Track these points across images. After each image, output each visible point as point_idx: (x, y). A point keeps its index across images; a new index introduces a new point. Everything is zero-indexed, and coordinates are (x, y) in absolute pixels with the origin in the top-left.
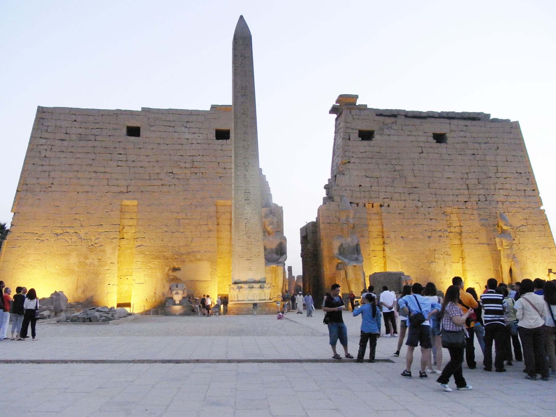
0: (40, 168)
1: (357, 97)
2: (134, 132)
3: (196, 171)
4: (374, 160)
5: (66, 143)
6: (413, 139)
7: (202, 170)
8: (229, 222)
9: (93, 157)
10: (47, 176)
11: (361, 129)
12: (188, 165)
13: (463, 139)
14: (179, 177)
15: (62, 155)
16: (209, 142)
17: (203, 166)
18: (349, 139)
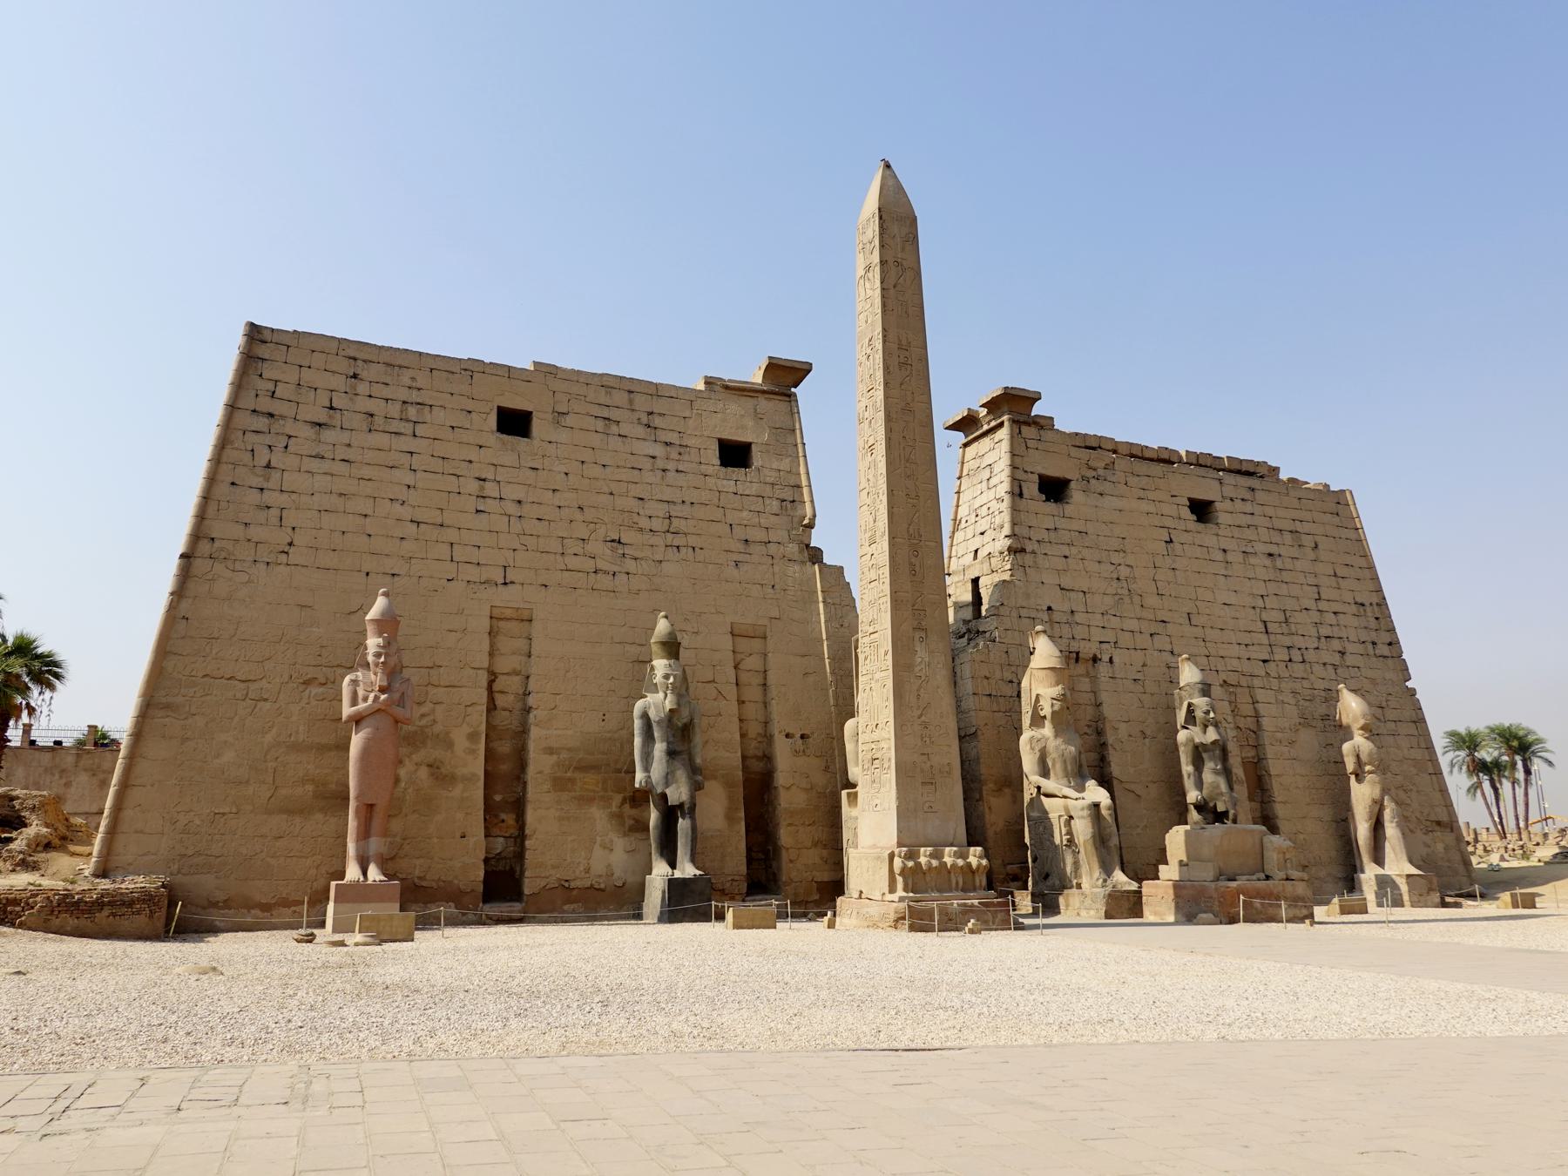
0: (254, 497)
1: (1033, 398)
2: (514, 423)
3: (678, 541)
4: (1074, 550)
5: (329, 435)
6: (1152, 509)
7: (692, 541)
8: (758, 680)
9: (409, 478)
10: (276, 521)
11: (1043, 472)
12: (657, 524)
13: (1248, 520)
14: (637, 554)
15: (315, 465)
18: (1021, 495)
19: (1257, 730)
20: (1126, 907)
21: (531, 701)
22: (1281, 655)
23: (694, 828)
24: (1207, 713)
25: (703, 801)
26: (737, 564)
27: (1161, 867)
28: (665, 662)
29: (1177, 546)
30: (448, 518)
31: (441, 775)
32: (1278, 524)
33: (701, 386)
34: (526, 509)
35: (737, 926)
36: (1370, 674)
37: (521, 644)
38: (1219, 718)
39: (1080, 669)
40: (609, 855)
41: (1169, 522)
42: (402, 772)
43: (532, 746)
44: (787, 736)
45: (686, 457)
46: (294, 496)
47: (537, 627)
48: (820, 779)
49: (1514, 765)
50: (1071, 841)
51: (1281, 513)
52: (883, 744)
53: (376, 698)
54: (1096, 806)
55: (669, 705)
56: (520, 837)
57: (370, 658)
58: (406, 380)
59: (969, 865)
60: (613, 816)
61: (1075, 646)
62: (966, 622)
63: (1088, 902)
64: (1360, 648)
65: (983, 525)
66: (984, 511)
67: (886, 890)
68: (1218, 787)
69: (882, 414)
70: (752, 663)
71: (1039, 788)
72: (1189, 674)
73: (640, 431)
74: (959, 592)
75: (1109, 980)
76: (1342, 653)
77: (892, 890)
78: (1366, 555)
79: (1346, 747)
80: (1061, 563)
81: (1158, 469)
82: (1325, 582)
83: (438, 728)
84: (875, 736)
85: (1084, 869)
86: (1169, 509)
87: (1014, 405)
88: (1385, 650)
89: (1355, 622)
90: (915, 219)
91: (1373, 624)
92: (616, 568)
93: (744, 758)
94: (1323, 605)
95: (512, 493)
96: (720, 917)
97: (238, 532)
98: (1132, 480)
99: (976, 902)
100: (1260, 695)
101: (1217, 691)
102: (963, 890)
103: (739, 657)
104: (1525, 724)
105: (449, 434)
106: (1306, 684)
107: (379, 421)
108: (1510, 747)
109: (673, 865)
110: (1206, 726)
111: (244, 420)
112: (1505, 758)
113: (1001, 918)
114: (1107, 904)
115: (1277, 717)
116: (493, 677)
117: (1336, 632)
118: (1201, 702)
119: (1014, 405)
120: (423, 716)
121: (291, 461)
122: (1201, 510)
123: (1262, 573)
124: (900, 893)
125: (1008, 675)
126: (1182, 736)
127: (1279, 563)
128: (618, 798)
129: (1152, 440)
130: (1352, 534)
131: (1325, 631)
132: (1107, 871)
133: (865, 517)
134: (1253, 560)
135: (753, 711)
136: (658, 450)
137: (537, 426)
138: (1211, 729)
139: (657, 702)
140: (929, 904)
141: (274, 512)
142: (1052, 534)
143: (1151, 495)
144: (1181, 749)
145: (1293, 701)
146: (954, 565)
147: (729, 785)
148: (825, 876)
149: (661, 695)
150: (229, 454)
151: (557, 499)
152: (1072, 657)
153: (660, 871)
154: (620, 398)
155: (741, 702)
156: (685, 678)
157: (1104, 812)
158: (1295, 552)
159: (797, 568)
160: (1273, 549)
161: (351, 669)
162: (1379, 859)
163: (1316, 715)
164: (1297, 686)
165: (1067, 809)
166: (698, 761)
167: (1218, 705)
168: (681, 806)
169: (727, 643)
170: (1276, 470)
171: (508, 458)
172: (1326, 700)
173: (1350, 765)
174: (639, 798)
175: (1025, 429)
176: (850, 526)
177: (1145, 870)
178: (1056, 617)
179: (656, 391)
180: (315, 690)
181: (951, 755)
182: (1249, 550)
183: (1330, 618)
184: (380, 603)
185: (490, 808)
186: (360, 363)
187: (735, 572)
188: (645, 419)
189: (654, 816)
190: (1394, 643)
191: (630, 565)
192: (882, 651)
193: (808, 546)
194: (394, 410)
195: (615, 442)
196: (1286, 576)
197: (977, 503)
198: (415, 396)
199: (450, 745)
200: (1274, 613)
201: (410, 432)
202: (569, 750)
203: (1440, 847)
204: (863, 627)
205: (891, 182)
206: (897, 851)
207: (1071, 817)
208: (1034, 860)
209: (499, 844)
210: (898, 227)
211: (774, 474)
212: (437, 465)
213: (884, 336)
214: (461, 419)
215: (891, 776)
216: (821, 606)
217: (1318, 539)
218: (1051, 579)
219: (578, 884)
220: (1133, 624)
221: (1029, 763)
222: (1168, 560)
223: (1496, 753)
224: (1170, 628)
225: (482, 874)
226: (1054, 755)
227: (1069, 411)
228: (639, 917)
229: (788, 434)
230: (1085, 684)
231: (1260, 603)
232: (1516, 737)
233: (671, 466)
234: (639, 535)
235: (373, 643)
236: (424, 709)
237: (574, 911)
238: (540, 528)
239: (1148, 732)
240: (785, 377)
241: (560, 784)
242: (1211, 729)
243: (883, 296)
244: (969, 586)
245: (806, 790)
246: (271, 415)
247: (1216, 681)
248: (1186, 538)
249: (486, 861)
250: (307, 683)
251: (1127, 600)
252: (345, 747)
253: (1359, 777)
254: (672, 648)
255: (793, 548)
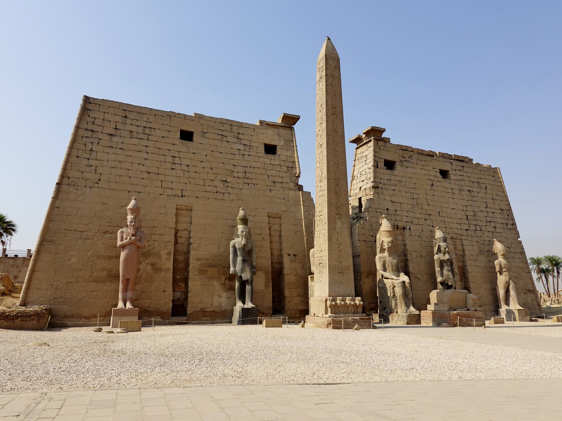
0: (85, 162)
1: (383, 131)
2: (187, 136)
3: (249, 181)
4: (397, 188)
5: (115, 139)
6: (425, 172)
7: (254, 181)
8: (278, 234)
9: (146, 156)
10: (94, 171)
12: (240, 175)
13: (461, 178)
15: (109, 150)
16: (258, 154)
17: (254, 178)
18: (377, 167)
19: (463, 255)
20: (414, 320)
21: (191, 241)
22: (472, 228)
23: (252, 289)
24: (445, 248)
25: (255, 279)
26: (270, 190)
27: (428, 305)
28: (242, 226)
29: (435, 187)
30: (161, 171)
31: (156, 268)
32: (472, 179)
33: (258, 124)
34: (191, 168)
35: (267, 326)
36: (505, 235)
37: (188, 219)
38: (450, 251)
39: (399, 232)
40: (220, 299)
41: (432, 178)
42: (141, 267)
43: (191, 258)
44: (288, 255)
45: (252, 150)
46: (101, 162)
47: (194, 213)
48: (300, 271)
49: (553, 270)
50: (394, 296)
51: (473, 175)
52: (324, 258)
53: (130, 238)
54: (404, 282)
55: (243, 243)
56: (186, 292)
57: (128, 223)
58: (145, 119)
59: (356, 304)
60: (221, 284)
61: (396, 223)
62: (356, 214)
63: (400, 318)
64: (501, 226)
65: (363, 178)
66: (364, 173)
67: (324, 313)
68: (449, 276)
69: (325, 133)
70: (276, 227)
71: (382, 276)
72: (439, 234)
73: (235, 140)
74: (354, 202)
75: (410, 351)
76: (495, 227)
77: (326, 313)
78: (504, 192)
79: (496, 262)
80: (392, 192)
81: (429, 158)
82: (489, 201)
83: (155, 250)
84: (321, 254)
85: (399, 306)
86: (432, 173)
87: (375, 133)
88: (511, 227)
89: (499, 216)
90: (339, 59)
91: (506, 217)
92: (224, 191)
93: (272, 263)
94: (488, 210)
95: (185, 162)
96: (261, 323)
97: (79, 175)
98: (419, 162)
99: (358, 318)
100: (465, 242)
101: (449, 241)
102: (354, 313)
103: (271, 225)
104: (558, 256)
105: (162, 140)
106: (482, 239)
107: (135, 134)
108: (552, 264)
109: (244, 303)
110: (445, 254)
111: (82, 132)
112: (550, 268)
113: (367, 324)
114: (408, 319)
115: (471, 250)
116: (177, 231)
117: (493, 220)
118: (443, 245)
119: (375, 133)
120: (149, 246)
121: (100, 149)
122: (444, 174)
123: (466, 197)
124: (329, 314)
125: (371, 234)
126: (436, 257)
127: (472, 194)
128: (224, 278)
129: (427, 148)
130: (499, 184)
131: (489, 219)
132: (408, 307)
133: (318, 172)
134: (463, 193)
135: (276, 245)
136: (241, 147)
137: (195, 137)
138: (447, 255)
139: (239, 242)
140: (340, 318)
141: (93, 168)
142: (389, 182)
143: (426, 168)
144: (436, 262)
145: (477, 245)
146: (352, 193)
147: (266, 273)
148: (302, 308)
149: (240, 239)
150: (76, 145)
151: (203, 165)
152: (395, 227)
153: (239, 305)
154: (227, 127)
155: (271, 242)
156: (250, 233)
157: (407, 285)
158: (478, 190)
159: (293, 192)
160: (470, 189)
161: (122, 227)
162: (507, 304)
163: (485, 250)
164: (478, 239)
165: (393, 283)
166: (254, 264)
167: (450, 246)
168: (247, 280)
169: (266, 220)
170: (471, 160)
171: (184, 149)
172: (489, 245)
173: (497, 269)
174: (232, 278)
175: (379, 142)
176: (313, 177)
177: (422, 307)
178: (390, 212)
179: (241, 125)
180: (108, 235)
181: (350, 262)
182: (461, 189)
183: (491, 214)
184: (133, 202)
185: (175, 281)
186: (127, 112)
187: (270, 193)
188: (236, 136)
189: (237, 284)
190: (514, 224)
191: (230, 190)
192: (324, 223)
193: (297, 184)
194: (141, 130)
195: (225, 144)
196: (475, 199)
197: (361, 170)
198: (148, 125)
199: (160, 257)
200: (470, 212)
201: (147, 138)
202: (205, 259)
203: (530, 299)
204: (317, 214)
205: (330, 45)
206: (328, 298)
207: (394, 287)
208: (380, 302)
209: (178, 294)
210: (332, 62)
211: (285, 157)
212: (157, 151)
213: (326, 103)
214: (166, 134)
215: (327, 270)
216: (302, 206)
217: (487, 185)
218: (388, 198)
219: (208, 310)
220: (418, 216)
221: (379, 266)
222: (432, 192)
223: (547, 266)
224: (432, 217)
225: (171, 306)
226: (389, 263)
227: (395, 136)
228: (231, 322)
229: (291, 142)
230: (400, 237)
231: (465, 208)
232: (554, 260)
233: (246, 153)
234: (234, 179)
235: (130, 217)
236: (150, 243)
237: (206, 320)
238: (196, 176)
239: (423, 255)
240: (290, 121)
241: (202, 272)
242: (447, 255)
243: (326, 88)
244: (358, 201)
245: (295, 275)
246: (93, 131)
247: (448, 237)
248: (438, 184)
249: (173, 301)
250: (105, 233)
251: (416, 206)
252: (119, 257)
253: (501, 273)
254: (245, 221)
255: (292, 185)
